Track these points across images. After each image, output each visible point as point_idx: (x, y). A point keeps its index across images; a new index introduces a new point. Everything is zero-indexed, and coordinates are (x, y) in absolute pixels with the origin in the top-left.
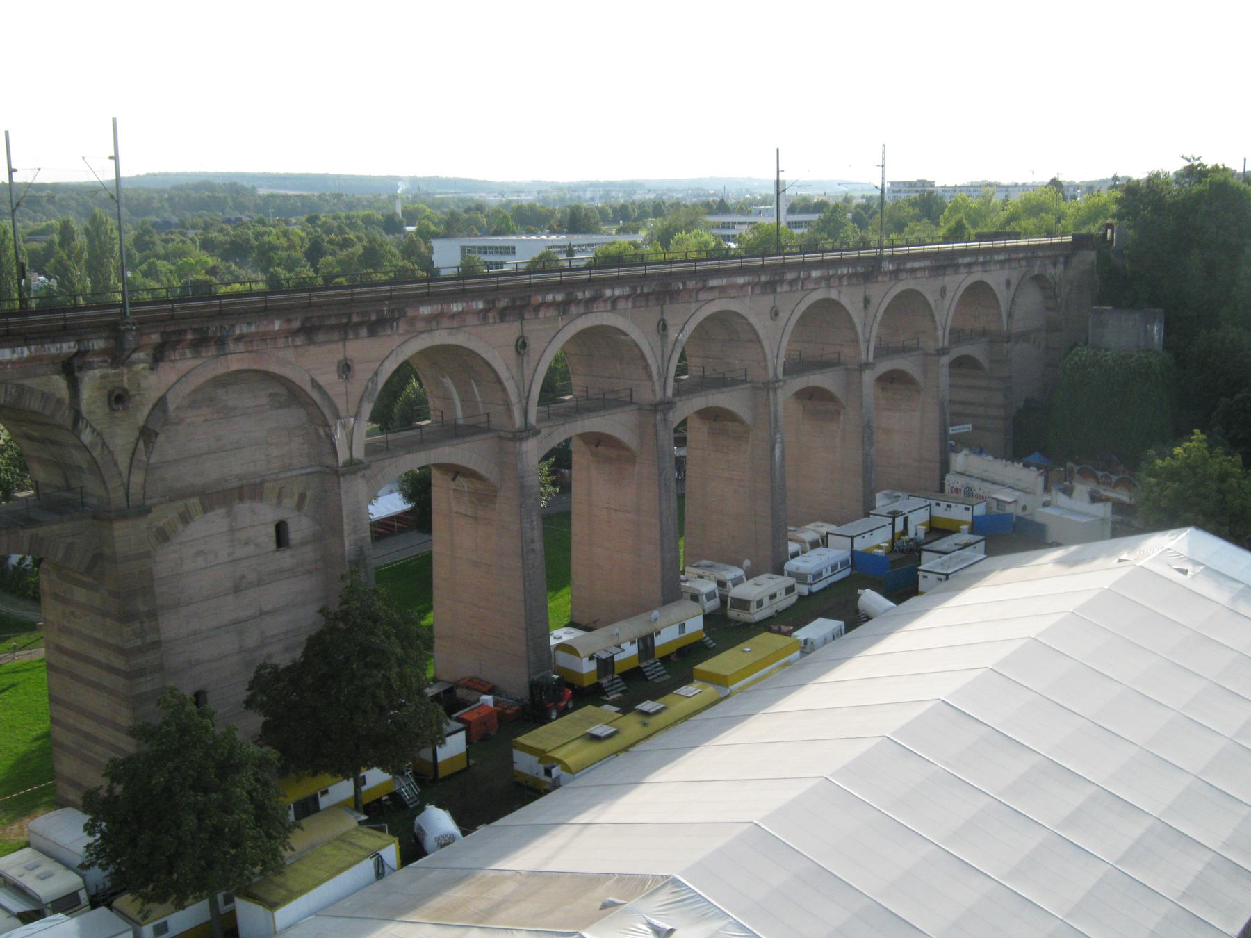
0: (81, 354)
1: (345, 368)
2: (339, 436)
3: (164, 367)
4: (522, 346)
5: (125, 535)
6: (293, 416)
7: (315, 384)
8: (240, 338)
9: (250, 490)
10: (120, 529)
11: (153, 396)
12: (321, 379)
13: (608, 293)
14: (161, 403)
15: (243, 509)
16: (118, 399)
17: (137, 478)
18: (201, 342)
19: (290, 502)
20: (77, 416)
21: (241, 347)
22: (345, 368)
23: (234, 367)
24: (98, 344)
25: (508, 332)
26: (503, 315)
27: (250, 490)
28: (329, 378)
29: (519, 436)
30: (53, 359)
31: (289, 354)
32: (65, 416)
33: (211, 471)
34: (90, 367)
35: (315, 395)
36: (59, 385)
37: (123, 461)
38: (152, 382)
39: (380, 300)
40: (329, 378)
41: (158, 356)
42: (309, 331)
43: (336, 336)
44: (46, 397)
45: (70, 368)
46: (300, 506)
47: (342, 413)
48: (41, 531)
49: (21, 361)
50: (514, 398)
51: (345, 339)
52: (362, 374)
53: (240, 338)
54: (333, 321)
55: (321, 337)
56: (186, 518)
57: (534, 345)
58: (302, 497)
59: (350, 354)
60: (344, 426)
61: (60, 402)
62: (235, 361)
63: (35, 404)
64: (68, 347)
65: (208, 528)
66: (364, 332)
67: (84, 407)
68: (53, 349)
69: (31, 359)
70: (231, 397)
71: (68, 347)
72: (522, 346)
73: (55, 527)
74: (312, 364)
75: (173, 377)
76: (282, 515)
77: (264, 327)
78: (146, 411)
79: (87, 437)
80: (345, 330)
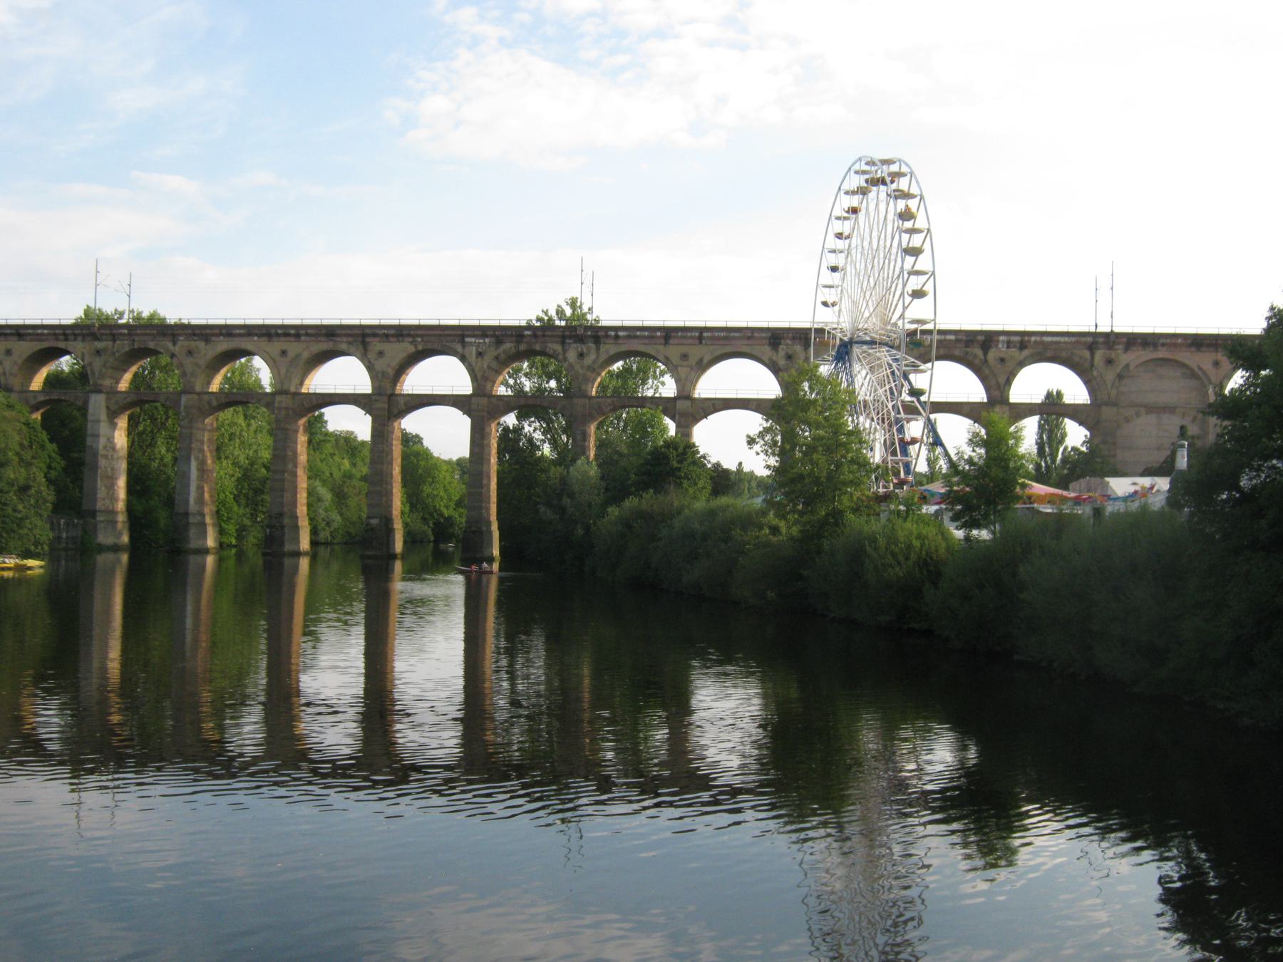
3: (1129, 353)
7: (1200, 368)
8: (1163, 345)
9: (1170, 409)
10: (1104, 409)
11: (1124, 363)
14: (1127, 366)
15: (1166, 418)
16: (1109, 362)
17: (1114, 392)
20: (1092, 365)
27: (1170, 409)
28: (1208, 366)
30: (1085, 343)
32: (1087, 365)
35: (1200, 373)
36: (1087, 354)
40: (1208, 366)
44: (1081, 357)
49: (1071, 343)
53: (1163, 345)
55: (1204, 349)
56: (1138, 415)
76: (1183, 423)
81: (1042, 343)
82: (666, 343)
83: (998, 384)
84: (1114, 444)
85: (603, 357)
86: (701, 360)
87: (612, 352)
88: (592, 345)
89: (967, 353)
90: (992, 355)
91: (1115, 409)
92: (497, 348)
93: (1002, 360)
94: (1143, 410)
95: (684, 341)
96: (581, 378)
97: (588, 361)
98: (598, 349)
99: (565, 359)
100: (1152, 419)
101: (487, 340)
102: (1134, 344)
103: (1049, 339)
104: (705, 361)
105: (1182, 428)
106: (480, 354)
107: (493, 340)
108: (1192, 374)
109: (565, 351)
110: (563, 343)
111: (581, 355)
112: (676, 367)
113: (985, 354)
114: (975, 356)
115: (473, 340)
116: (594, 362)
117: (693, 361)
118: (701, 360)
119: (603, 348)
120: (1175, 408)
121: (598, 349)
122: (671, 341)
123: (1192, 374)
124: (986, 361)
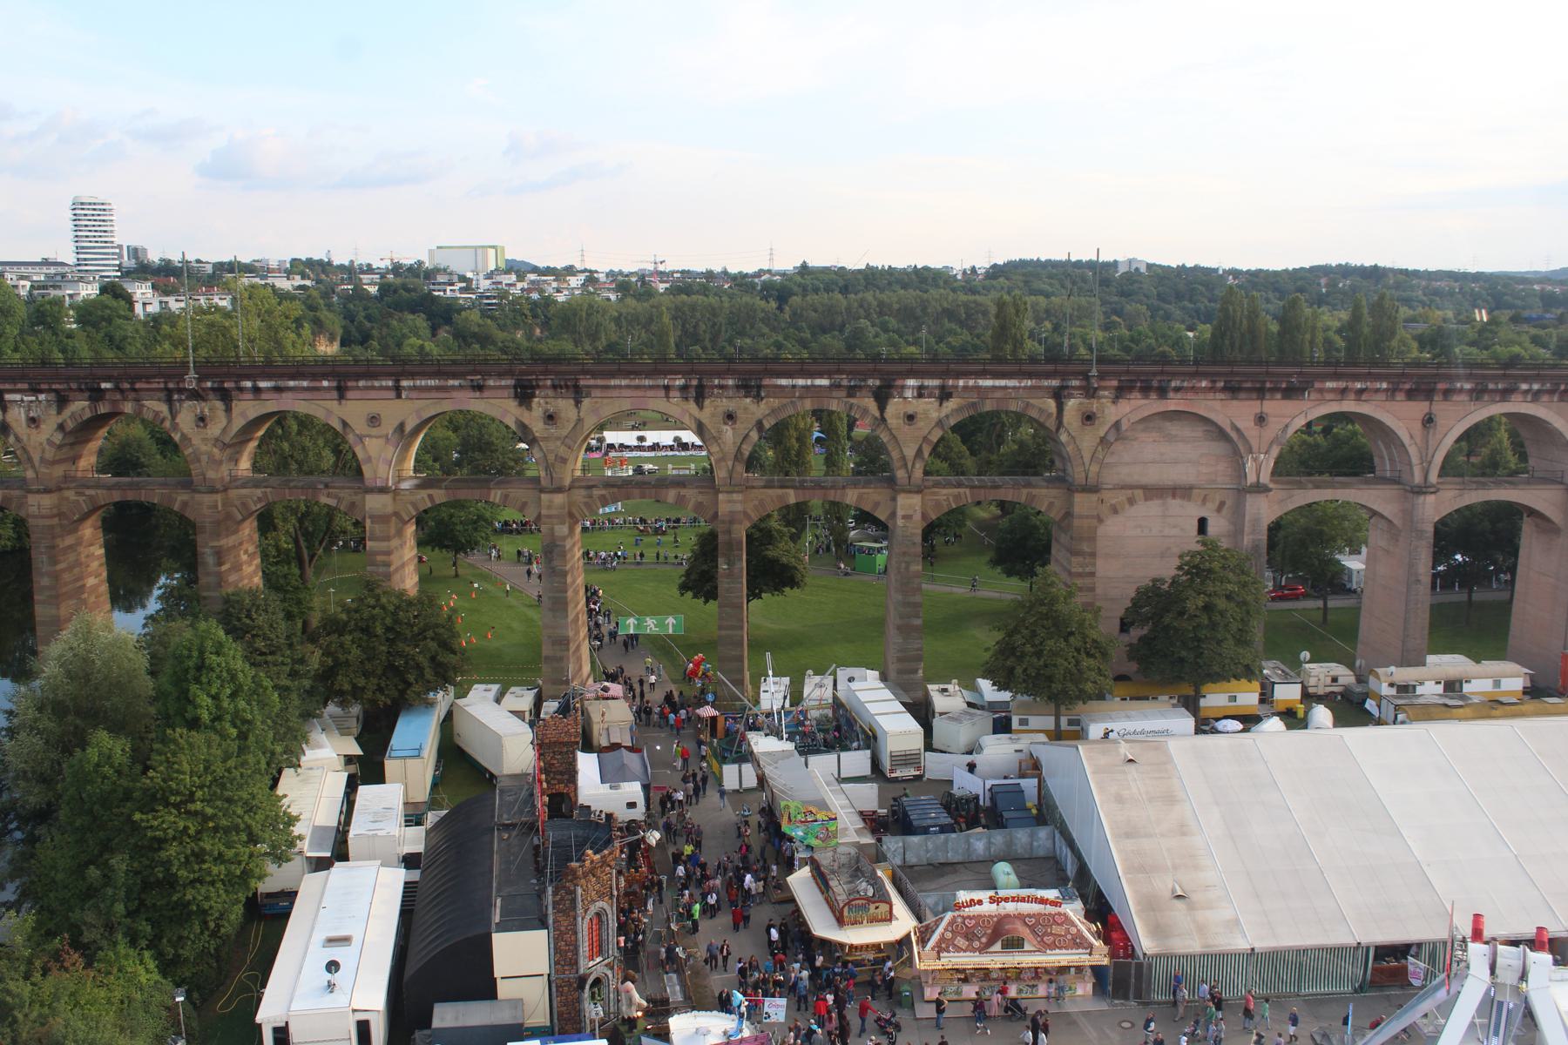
0: (1062, 388)
1: (1261, 419)
2: (1249, 465)
4: (1428, 421)
5: (1082, 503)
6: (1219, 448)
8: (1177, 389)
9: (1181, 491)
10: (1079, 498)
12: (1239, 425)
13: (1524, 387)
14: (1117, 425)
15: (1175, 504)
16: (1089, 418)
18: (1146, 390)
19: (1212, 506)
21: (1179, 395)
22: (1261, 419)
23: (1172, 408)
24: (1075, 383)
25: (1419, 408)
26: (1411, 395)
27: (1181, 491)
28: (1246, 424)
29: (1422, 490)
31: (1217, 405)
33: (1154, 475)
34: (1070, 396)
35: (1234, 435)
36: (1051, 404)
37: (1087, 457)
38: (1113, 411)
39: (1290, 375)
41: (1121, 392)
42: (1233, 390)
43: (1254, 395)
44: (1041, 411)
45: (1059, 395)
46: (1219, 510)
47: (1255, 449)
48: (1035, 491)
49: (1025, 388)
50: (1415, 460)
51: (1262, 398)
52: (1273, 427)
53: (1177, 389)
54: (1249, 385)
55: (1242, 395)
56: (1131, 501)
57: (1440, 421)
58: (1222, 504)
59: (1265, 410)
60: (1255, 460)
61: (1050, 415)
62: (1173, 403)
63: (1034, 414)
64: (1055, 383)
65: (1149, 510)
66: (1279, 396)
67: (1065, 420)
68: (1046, 383)
69: (1032, 387)
70: (1174, 428)
71: (1055, 383)
72: (1428, 421)
73: (1044, 491)
74: (1236, 413)
75: (1128, 409)
76: (1203, 514)
77: (1194, 382)
78: (1106, 428)
79: (1063, 438)
80: (1261, 393)
81: (978, 388)
82: (341, 397)
83: (903, 458)
84: (1093, 555)
85: (238, 423)
86: (401, 426)
87: (252, 415)
88: (219, 405)
89: (851, 406)
90: (894, 407)
91: (1094, 497)
92: (59, 413)
93: (911, 418)
94: (1139, 493)
95: (373, 394)
96: (204, 458)
97: (214, 430)
98: (228, 410)
99: (175, 426)
100: (1154, 507)
101: (42, 397)
102: (1131, 389)
103: (989, 383)
104: (408, 428)
105: (1202, 524)
106: (33, 421)
107: (52, 396)
108: (1221, 435)
109: (173, 415)
110: (169, 401)
111: (201, 420)
112: (361, 438)
113: (882, 408)
114: (865, 411)
115: (17, 397)
116: (224, 430)
117: (388, 427)
118: (401, 426)
119: (238, 407)
120: (1191, 488)
121: (228, 410)
122: (350, 394)
123: (1221, 435)
124: (883, 419)
